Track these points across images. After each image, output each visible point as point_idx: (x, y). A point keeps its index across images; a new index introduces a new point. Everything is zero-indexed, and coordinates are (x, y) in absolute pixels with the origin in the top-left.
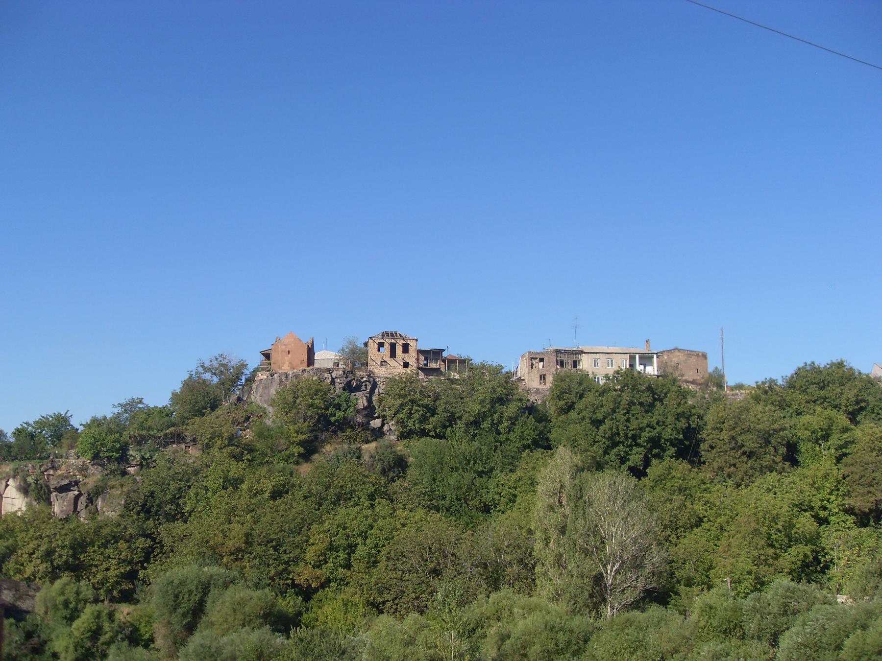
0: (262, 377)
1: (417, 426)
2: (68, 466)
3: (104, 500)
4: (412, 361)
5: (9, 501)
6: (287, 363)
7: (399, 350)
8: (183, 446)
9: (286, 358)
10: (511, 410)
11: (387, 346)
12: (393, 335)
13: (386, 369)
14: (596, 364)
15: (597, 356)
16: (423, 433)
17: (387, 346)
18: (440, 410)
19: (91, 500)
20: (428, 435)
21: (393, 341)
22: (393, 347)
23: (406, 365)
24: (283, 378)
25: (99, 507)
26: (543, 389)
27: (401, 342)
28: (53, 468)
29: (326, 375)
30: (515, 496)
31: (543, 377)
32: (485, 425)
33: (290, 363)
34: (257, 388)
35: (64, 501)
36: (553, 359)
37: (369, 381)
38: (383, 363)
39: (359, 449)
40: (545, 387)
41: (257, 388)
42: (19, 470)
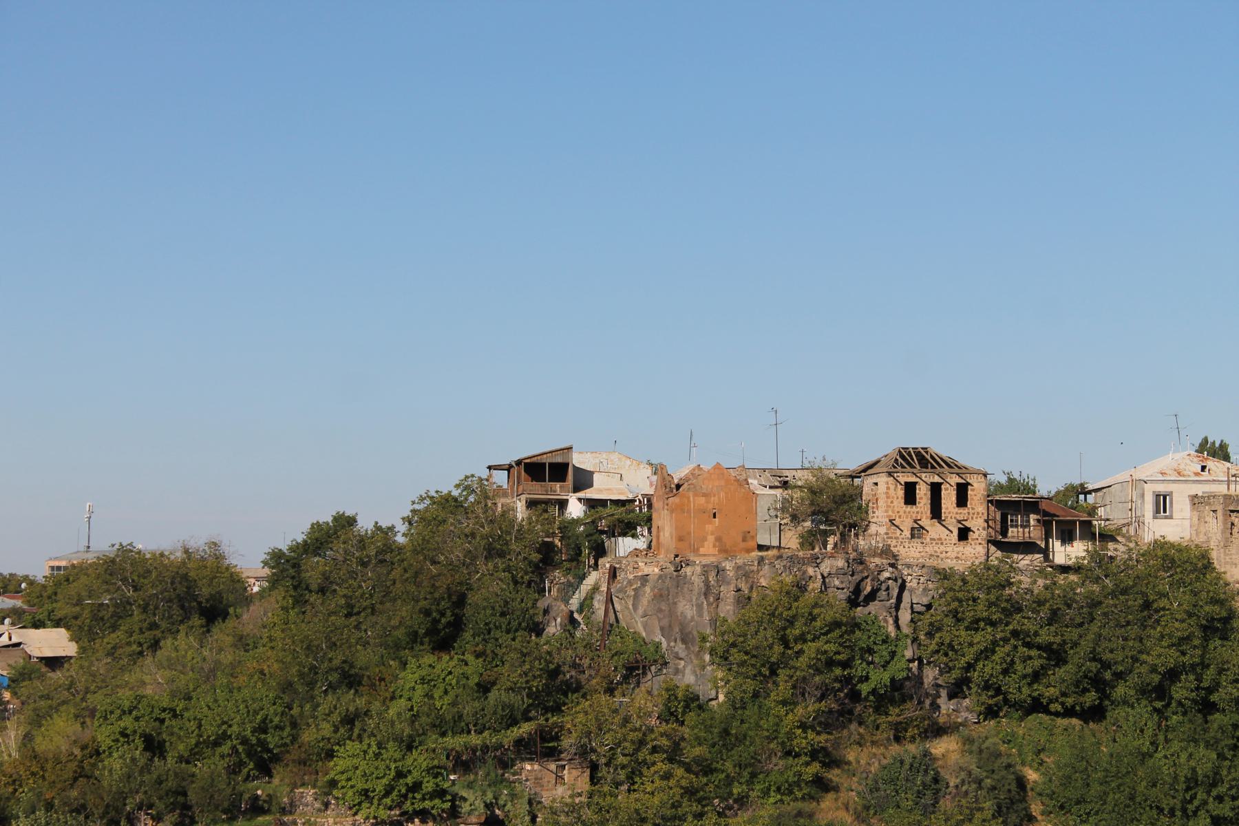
0: (647, 570)
1: (1026, 691)
6: (711, 538)
8: (553, 767)
9: (709, 528)
11: (923, 492)
12: (922, 459)
16: (1037, 706)
17: (923, 492)
20: (1046, 711)
21: (937, 479)
22: (936, 489)
23: (964, 534)
24: (712, 578)
29: (811, 571)
32: (1180, 692)
33: (718, 539)
34: (636, 597)
37: (896, 580)
38: (917, 532)
39: (926, 754)
41: (636, 597)
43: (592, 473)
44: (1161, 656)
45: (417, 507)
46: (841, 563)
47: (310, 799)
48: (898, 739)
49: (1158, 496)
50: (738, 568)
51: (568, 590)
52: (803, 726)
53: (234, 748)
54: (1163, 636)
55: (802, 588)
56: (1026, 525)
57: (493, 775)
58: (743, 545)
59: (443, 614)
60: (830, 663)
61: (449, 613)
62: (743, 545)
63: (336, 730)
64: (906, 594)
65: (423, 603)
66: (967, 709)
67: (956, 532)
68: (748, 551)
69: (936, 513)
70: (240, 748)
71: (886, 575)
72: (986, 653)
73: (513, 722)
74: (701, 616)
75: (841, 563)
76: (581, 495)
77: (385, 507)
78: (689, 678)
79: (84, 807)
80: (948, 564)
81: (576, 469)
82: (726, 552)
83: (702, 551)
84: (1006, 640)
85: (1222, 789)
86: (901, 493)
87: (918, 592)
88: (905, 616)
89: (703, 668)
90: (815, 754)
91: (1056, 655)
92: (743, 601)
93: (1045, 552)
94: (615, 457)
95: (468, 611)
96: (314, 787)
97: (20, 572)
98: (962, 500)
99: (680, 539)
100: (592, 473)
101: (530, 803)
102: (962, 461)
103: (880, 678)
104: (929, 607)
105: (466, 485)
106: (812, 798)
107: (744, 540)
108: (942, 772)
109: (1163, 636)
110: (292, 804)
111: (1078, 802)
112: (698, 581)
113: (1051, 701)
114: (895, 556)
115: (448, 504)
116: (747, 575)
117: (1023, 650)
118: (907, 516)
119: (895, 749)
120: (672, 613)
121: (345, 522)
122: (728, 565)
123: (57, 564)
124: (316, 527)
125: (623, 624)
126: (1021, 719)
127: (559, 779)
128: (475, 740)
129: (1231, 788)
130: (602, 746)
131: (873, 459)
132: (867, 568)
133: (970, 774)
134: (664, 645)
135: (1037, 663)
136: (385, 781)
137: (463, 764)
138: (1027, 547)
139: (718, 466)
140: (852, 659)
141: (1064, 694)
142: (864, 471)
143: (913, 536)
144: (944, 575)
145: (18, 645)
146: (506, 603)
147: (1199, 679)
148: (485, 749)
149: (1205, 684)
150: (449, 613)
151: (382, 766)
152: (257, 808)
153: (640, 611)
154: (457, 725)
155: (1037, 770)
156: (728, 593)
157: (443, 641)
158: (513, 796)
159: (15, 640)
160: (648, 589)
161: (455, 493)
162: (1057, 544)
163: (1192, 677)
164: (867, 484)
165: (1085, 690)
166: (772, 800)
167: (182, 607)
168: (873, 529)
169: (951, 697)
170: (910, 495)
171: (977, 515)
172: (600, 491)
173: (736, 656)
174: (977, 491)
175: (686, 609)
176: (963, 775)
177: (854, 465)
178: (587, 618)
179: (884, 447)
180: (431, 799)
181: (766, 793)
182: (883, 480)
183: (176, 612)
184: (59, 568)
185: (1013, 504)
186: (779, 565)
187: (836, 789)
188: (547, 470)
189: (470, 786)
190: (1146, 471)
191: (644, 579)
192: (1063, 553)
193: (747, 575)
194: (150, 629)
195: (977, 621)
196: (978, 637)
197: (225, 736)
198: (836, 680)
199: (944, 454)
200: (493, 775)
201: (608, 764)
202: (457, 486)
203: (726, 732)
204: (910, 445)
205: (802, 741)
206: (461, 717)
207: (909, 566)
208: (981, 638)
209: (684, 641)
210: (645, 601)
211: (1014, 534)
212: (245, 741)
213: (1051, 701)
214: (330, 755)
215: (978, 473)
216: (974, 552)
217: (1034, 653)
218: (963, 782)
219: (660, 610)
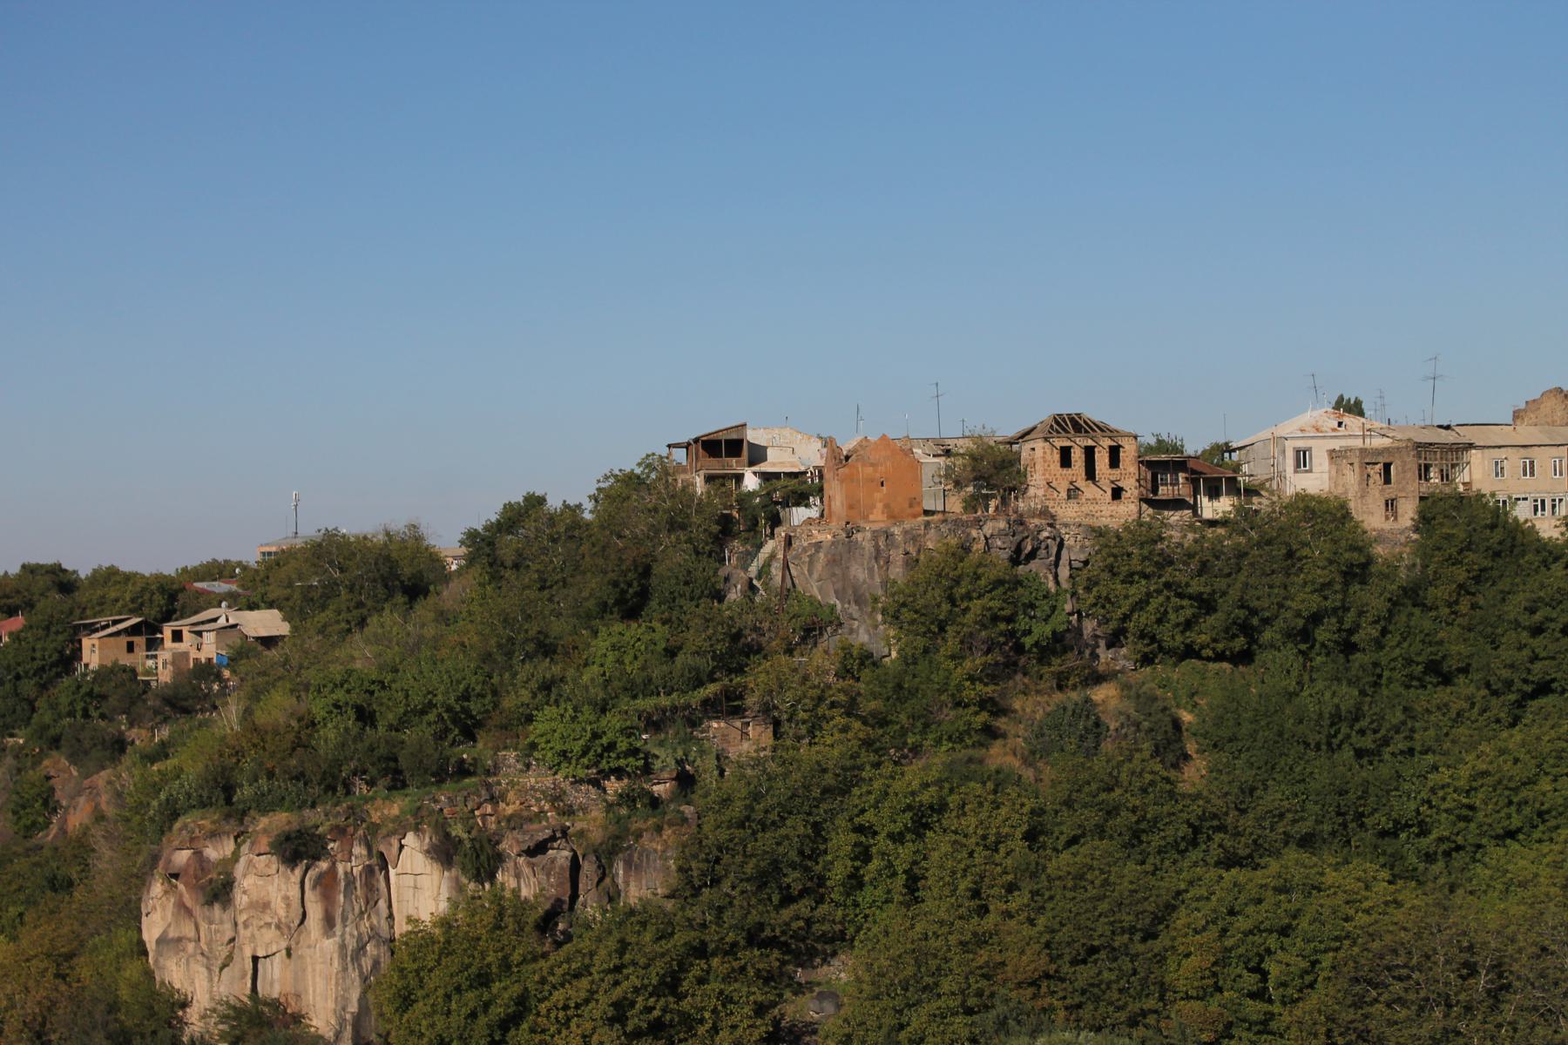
0: (820, 537)
2: (523, 792)
3: (628, 864)
4: (1130, 485)
5: (409, 880)
6: (880, 506)
7: (1102, 459)
8: (738, 724)
9: (878, 495)
10: (1372, 599)
11: (1077, 456)
12: (1076, 424)
13: (1089, 508)
14: (1499, 471)
15: (1502, 453)
16: (1190, 652)
17: (1077, 456)
18: (1225, 605)
19: (603, 872)
20: (1198, 656)
21: (1090, 443)
22: (1089, 452)
23: (1117, 493)
25: (620, 881)
26: (1391, 531)
27: (1107, 443)
28: (493, 799)
29: (974, 533)
30: (1471, 808)
31: (1390, 504)
32: (1323, 634)
33: (887, 506)
34: (811, 563)
35: (548, 875)
36: (1412, 463)
38: (1073, 493)
39: (1087, 700)
40: (1396, 526)
41: (811, 563)
42: (424, 813)
43: (765, 448)
44: (1305, 601)
45: (602, 485)
46: (1002, 525)
47: (512, 761)
48: (1060, 688)
49: (1298, 452)
50: (906, 532)
51: (749, 556)
52: (972, 679)
53: (439, 715)
54: (1306, 583)
55: (966, 549)
56: (1175, 483)
57: (682, 733)
58: (909, 511)
59: (630, 585)
60: (995, 619)
61: (635, 584)
62: (909, 511)
63: (534, 696)
64: (1064, 552)
65: (611, 576)
66: (1125, 657)
67: (1109, 492)
68: (915, 516)
69: (1090, 474)
70: (446, 716)
71: (1045, 534)
72: (1141, 605)
73: (699, 683)
74: (871, 576)
75: (1002, 525)
76: (756, 468)
77: (572, 486)
78: (863, 637)
79: (302, 774)
80: (1103, 521)
81: (752, 446)
82: (894, 517)
83: (872, 517)
84: (1159, 592)
85: (1363, 723)
86: (1057, 457)
87: (1076, 548)
88: (1064, 572)
89: (876, 627)
90: (983, 703)
91: (1206, 605)
92: (911, 563)
93: (1194, 508)
94: (787, 432)
95: (654, 581)
96: (516, 749)
97: (234, 558)
98: (1114, 461)
99: (851, 507)
100: (765, 448)
101: (718, 758)
102: (1113, 425)
103: (1042, 631)
104: (1086, 563)
105: (647, 463)
106: (982, 745)
107: (911, 506)
108: (1103, 717)
109: (1306, 583)
110: (496, 766)
111: (1230, 740)
112: (868, 546)
113: (1202, 647)
114: (1053, 517)
115: (630, 482)
116: (914, 539)
117: (1176, 601)
118: (1062, 478)
119: (1058, 697)
120: (845, 577)
121: (535, 502)
122: (896, 530)
123: (267, 549)
124: (508, 507)
125: (799, 588)
126: (1175, 665)
127: (745, 735)
128: (664, 701)
129: (1372, 722)
130: (784, 702)
131: (1030, 426)
132: (1027, 529)
133: (1128, 717)
134: (839, 607)
135: (1189, 612)
136: (582, 742)
137: (654, 724)
138: (1177, 504)
139: (884, 437)
140: (1015, 614)
141: (1215, 640)
142: (1022, 437)
143: (1069, 497)
144: (1099, 533)
145: (235, 626)
146: (689, 572)
147: (1341, 621)
148: (674, 709)
149: (1346, 626)
150: (635, 584)
151: (578, 728)
152: (463, 771)
153: (815, 576)
154: (646, 688)
155: (1191, 712)
156: (897, 556)
157: (631, 609)
158: (702, 752)
159: (232, 622)
160: (822, 555)
161: (638, 471)
162: (1205, 500)
163: (1334, 620)
164: (1025, 450)
165: (1234, 636)
166: (944, 748)
167: (386, 586)
168: (1032, 491)
169: (1109, 647)
170: (1065, 458)
171: (1129, 475)
172: (774, 464)
173: (906, 615)
174: (1129, 452)
175: (858, 572)
176: (1122, 718)
177: (1011, 431)
178: (765, 584)
179: (1040, 414)
180: (625, 758)
181: (938, 742)
182: (1040, 445)
183: (381, 590)
184: (270, 554)
185: (1163, 463)
186: (944, 528)
187: (1004, 736)
188: (724, 447)
189: (661, 744)
190: (1288, 428)
191: (818, 545)
192: (1211, 508)
193: (914, 539)
194: (357, 607)
195: (1132, 574)
196: (1133, 590)
197: (431, 705)
198: (1001, 634)
199: (1096, 419)
200: (682, 733)
201: (789, 720)
202: (639, 465)
203: (899, 686)
204: (1064, 411)
205: (969, 693)
206: (650, 680)
207: (1066, 525)
208: (1136, 591)
209: (857, 602)
210: (819, 566)
211: (1164, 492)
212: (449, 709)
213: (1202, 647)
214: (530, 719)
215: (1128, 435)
216: (1128, 510)
217: (1185, 602)
218: (1122, 726)
219: (834, 575)
